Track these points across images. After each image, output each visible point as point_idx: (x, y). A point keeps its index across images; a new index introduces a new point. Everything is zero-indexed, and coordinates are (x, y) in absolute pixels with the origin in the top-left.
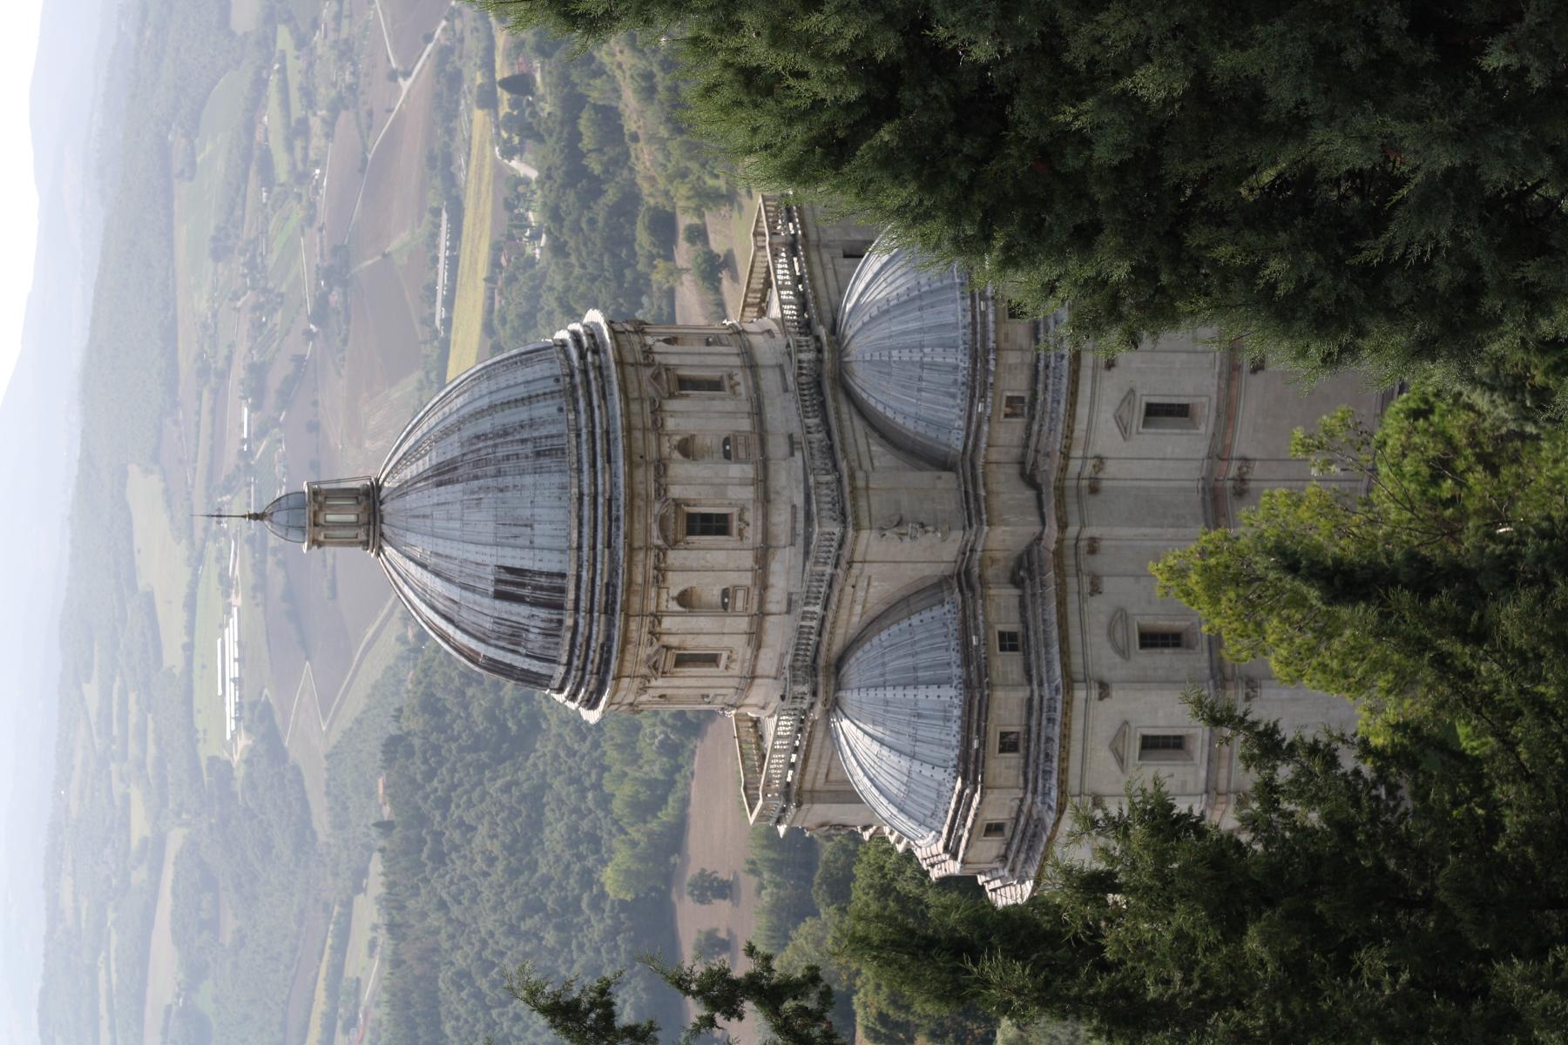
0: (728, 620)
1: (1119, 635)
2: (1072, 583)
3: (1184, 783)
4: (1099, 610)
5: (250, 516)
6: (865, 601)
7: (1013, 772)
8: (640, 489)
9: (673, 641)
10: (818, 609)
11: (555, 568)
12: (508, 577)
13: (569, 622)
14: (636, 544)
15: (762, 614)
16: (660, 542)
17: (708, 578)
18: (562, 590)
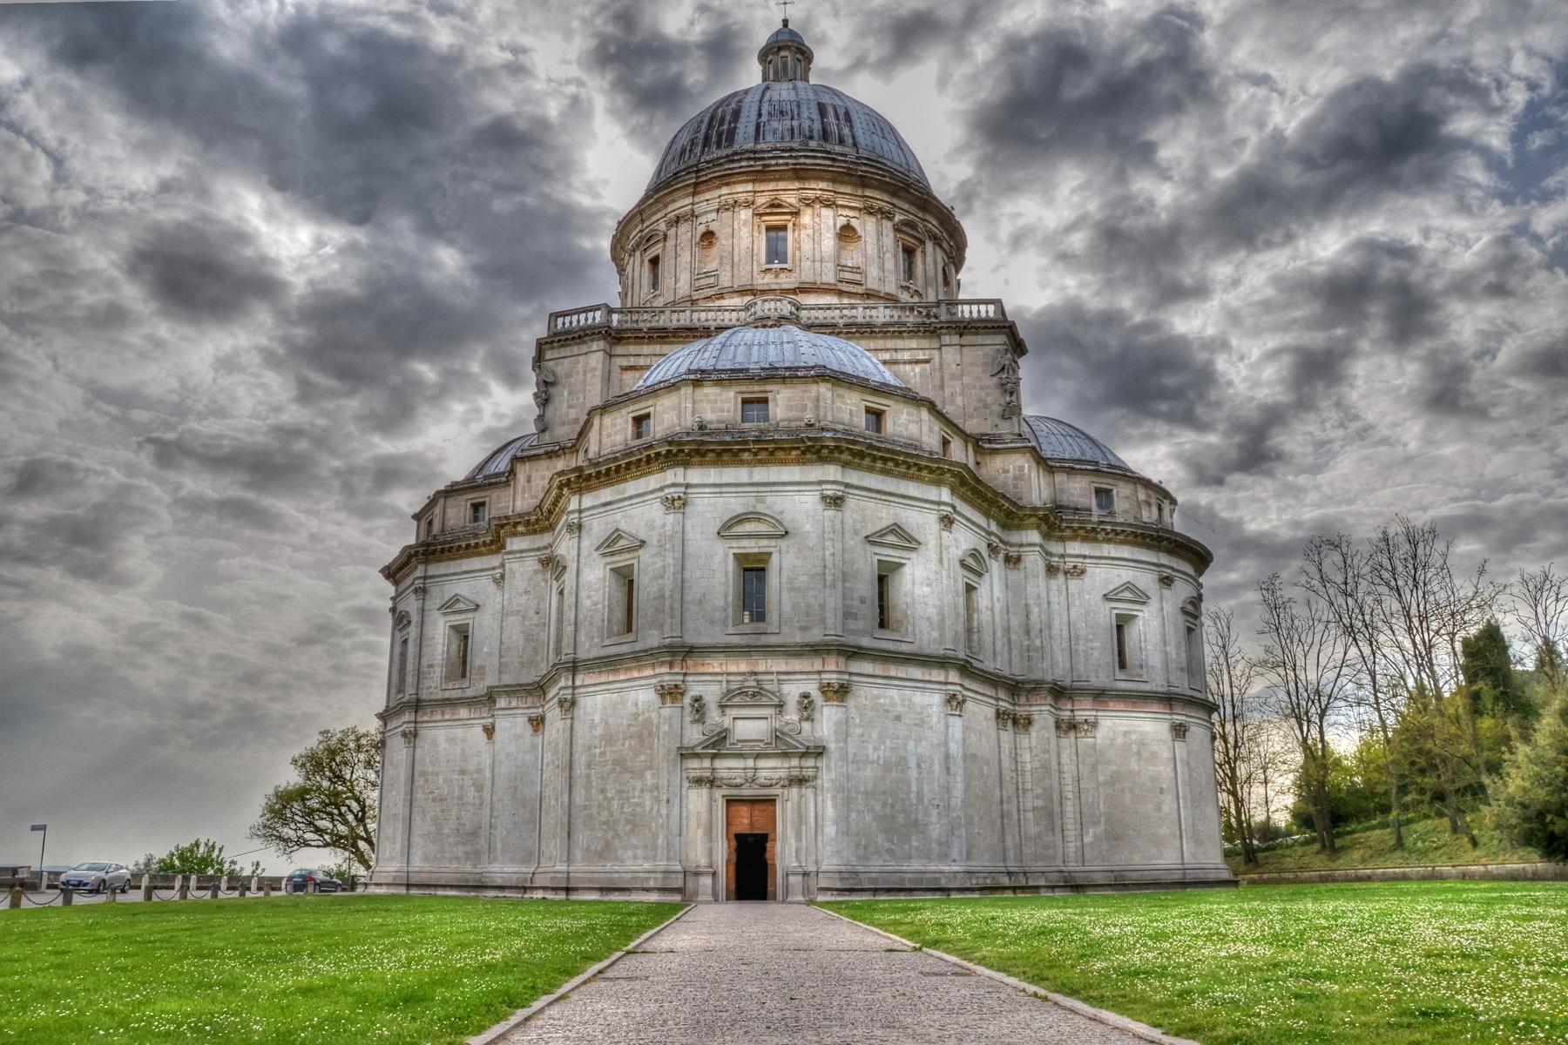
0: (831, 266)
1: (971, 562)
2: (994, 527)
3: (854, 616)
4: (985, 552)
5: (785, 23)
6: (896, 362)
7: (846, 418)
8: (929, 218)
9: (806, 217)
10: (882, 320)
11: (861, 140)
12: (841, 112)
13: (813, 144)
14: (895, 201)
15: (840, 293)
16: (898, 218)
17: (871, 250)
18: (841, 142)
